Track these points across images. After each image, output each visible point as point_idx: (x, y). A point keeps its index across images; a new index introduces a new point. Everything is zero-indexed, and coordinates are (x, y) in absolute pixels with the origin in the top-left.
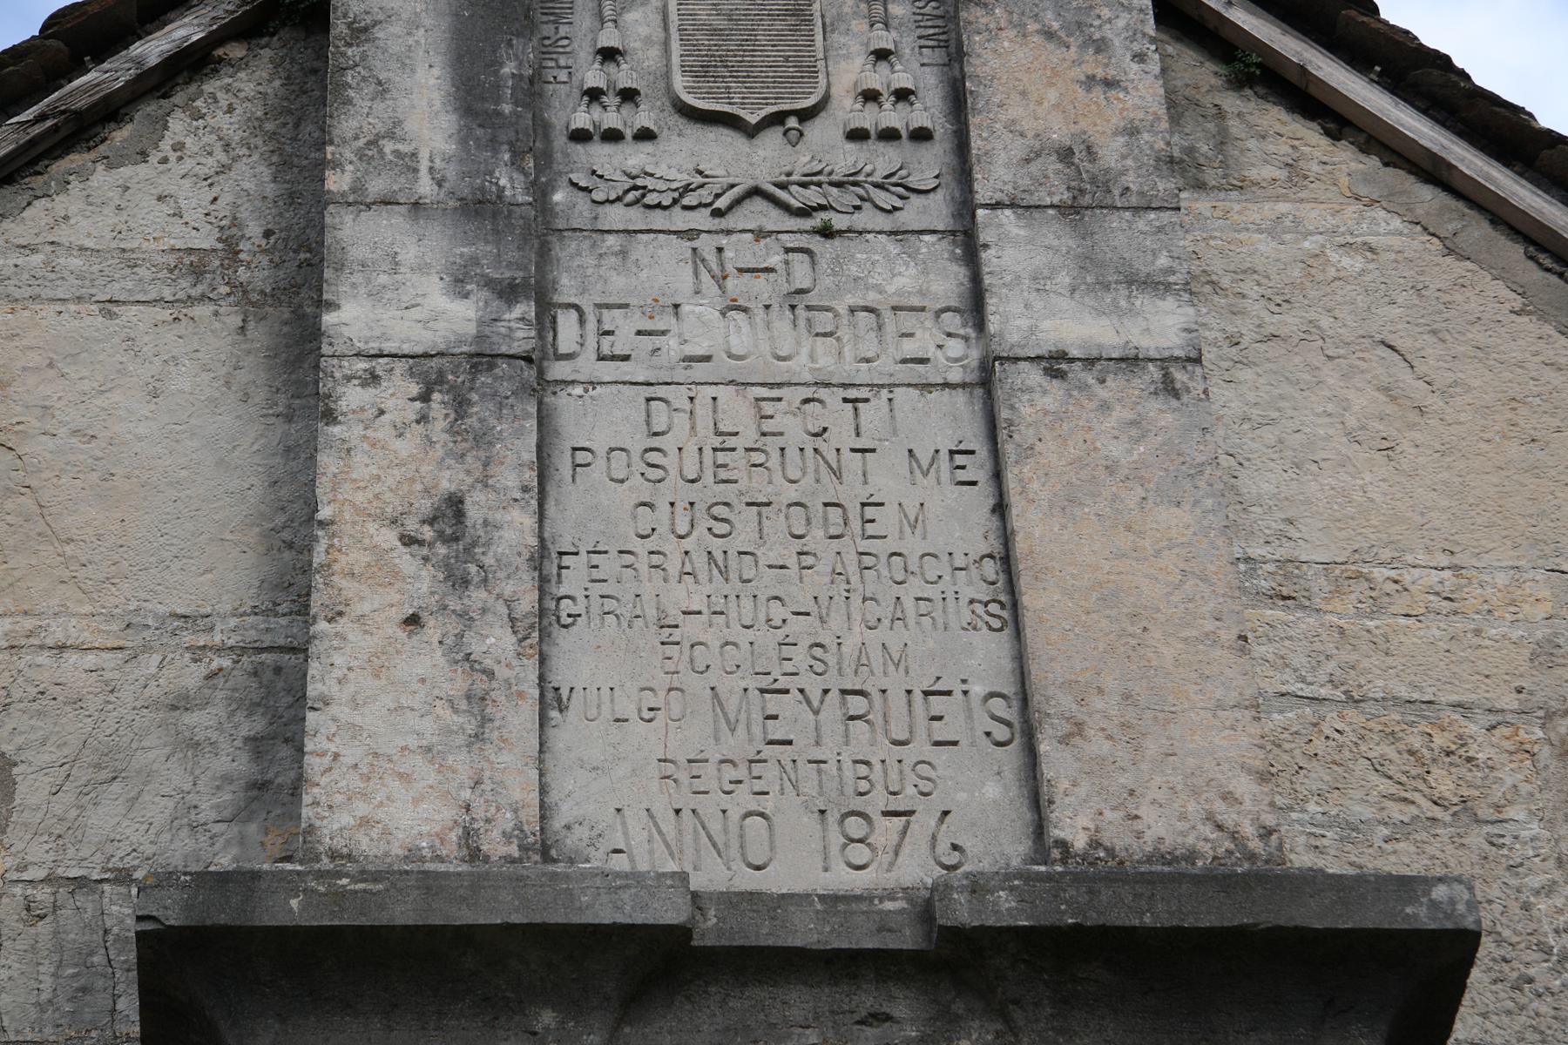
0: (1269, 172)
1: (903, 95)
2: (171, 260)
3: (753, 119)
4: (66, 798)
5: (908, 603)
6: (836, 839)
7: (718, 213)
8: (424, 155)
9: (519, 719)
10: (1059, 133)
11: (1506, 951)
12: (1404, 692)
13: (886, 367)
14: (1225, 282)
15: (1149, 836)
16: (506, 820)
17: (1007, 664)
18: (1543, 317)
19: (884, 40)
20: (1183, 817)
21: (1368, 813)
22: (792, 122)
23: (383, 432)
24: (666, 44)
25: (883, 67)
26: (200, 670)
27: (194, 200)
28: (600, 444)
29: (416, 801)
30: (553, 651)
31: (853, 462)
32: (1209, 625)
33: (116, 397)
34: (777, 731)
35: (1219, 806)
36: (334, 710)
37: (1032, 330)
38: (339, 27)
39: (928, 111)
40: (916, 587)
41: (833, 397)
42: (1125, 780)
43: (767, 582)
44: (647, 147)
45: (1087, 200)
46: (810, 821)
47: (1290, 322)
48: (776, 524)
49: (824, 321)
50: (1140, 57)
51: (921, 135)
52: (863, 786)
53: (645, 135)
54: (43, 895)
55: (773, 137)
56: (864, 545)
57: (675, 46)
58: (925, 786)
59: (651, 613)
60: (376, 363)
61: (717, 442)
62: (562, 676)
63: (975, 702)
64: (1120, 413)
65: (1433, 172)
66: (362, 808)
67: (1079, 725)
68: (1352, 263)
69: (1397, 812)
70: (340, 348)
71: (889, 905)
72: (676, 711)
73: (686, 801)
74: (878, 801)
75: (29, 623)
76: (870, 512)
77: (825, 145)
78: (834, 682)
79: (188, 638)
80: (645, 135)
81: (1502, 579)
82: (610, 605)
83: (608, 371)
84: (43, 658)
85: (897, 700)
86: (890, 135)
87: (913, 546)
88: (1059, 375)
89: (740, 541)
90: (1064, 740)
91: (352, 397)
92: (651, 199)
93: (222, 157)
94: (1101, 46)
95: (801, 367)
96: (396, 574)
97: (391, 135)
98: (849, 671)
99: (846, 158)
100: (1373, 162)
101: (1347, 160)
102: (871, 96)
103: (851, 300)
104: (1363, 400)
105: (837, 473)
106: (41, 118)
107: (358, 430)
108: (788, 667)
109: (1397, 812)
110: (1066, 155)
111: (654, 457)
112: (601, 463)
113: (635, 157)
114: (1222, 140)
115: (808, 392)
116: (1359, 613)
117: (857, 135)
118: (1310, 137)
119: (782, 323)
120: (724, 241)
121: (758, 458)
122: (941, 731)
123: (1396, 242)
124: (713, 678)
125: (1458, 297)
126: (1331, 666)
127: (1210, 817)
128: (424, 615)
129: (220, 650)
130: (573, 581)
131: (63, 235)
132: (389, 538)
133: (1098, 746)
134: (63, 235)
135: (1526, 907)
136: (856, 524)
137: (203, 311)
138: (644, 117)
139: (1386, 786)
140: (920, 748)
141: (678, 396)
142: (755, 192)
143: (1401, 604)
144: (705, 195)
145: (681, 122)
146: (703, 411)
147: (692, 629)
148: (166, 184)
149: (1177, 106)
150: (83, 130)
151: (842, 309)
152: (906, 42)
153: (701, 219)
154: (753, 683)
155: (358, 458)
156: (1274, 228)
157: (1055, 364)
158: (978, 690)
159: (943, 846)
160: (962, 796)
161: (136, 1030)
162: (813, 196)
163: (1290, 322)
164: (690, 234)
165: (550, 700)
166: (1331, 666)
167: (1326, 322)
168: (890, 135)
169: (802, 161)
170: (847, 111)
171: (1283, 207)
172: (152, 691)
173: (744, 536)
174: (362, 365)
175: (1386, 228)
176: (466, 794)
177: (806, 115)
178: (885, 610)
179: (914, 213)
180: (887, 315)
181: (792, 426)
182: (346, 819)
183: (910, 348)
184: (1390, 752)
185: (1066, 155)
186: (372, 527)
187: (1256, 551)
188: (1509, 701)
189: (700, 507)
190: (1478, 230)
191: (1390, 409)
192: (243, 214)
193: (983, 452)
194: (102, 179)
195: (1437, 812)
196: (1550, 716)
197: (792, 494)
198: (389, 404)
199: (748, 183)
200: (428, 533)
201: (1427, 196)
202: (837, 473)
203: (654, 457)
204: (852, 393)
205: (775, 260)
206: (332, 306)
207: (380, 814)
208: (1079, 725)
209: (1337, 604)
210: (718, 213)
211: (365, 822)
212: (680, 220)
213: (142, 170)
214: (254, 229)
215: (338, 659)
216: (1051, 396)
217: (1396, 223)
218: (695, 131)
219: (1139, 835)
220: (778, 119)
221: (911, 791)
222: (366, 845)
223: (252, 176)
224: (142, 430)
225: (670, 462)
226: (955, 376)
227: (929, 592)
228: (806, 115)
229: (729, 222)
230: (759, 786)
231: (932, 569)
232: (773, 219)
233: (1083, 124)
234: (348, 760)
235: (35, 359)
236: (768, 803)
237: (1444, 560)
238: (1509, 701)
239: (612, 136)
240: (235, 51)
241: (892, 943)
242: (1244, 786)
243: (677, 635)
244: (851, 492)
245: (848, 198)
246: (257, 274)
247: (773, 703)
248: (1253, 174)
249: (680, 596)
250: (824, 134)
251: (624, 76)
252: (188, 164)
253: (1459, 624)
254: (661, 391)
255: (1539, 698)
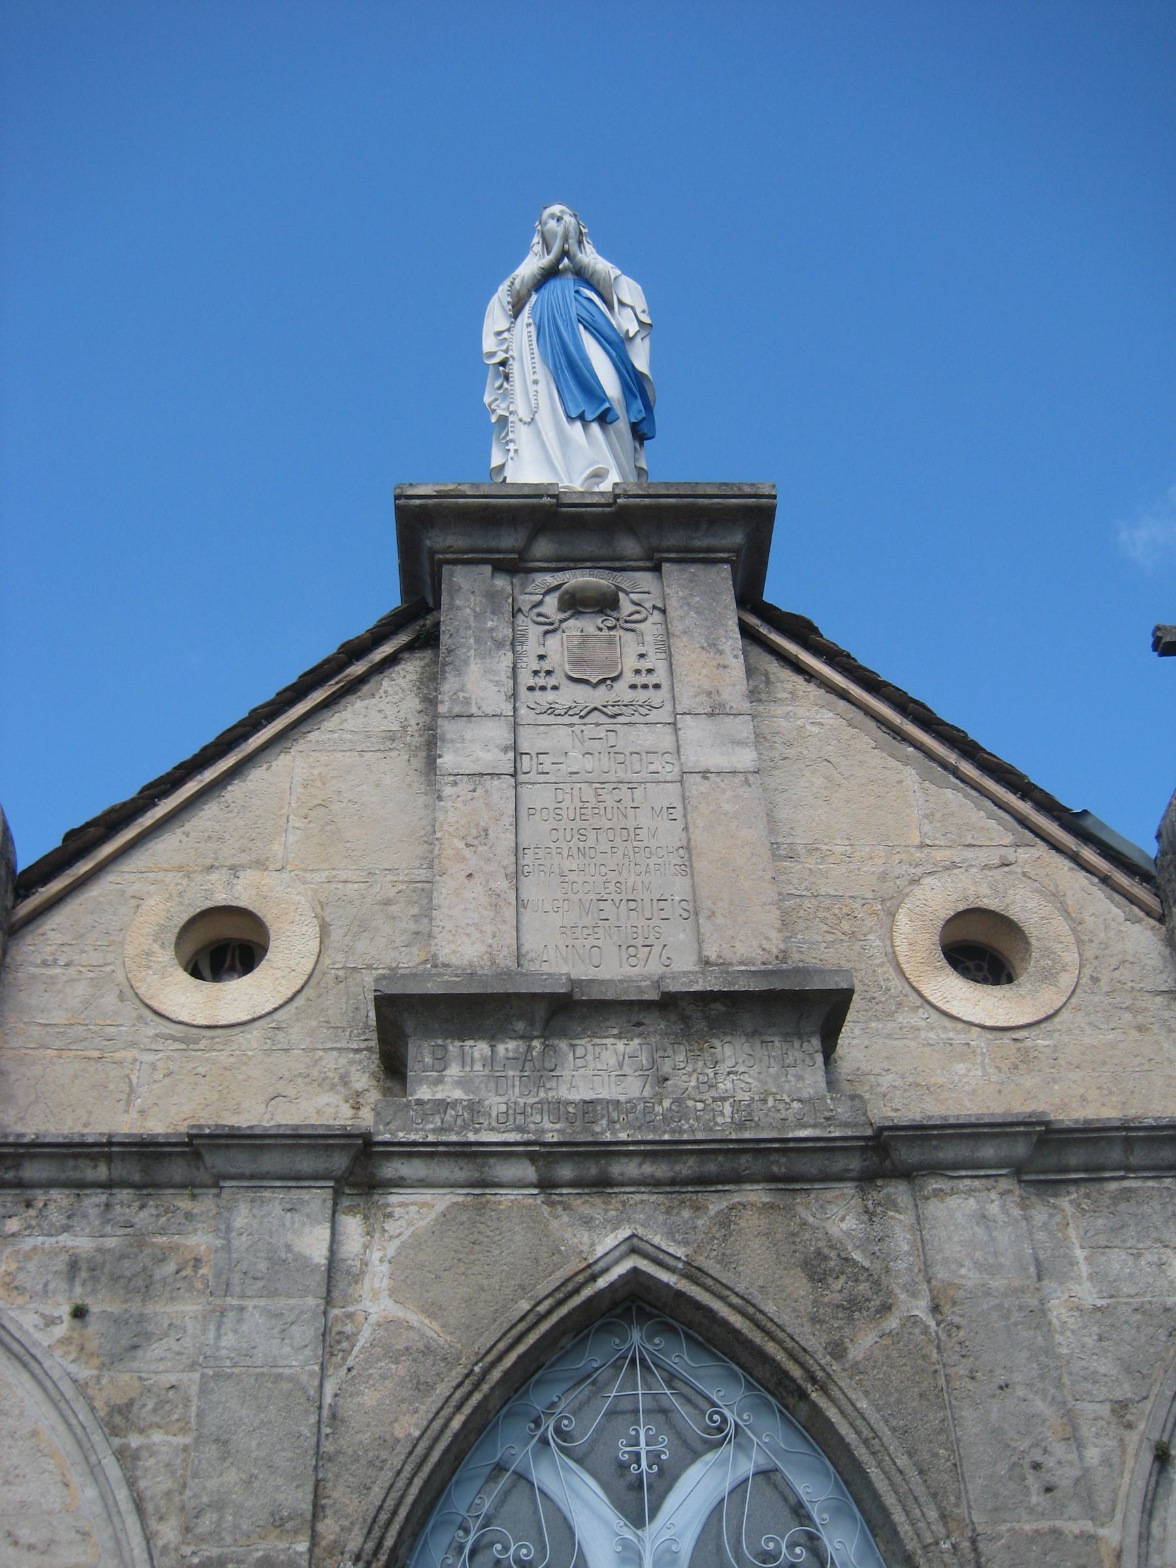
0: (785, 695)
1: (649, 671)
2: (383, 735)
3: (594, 681)
4: (348, 938)
5: (652, 866)
6: (625, 956)
7: (582, 717)
8: (473, 698)
9: (509, 913)
10: (707, 686)
11: (866, 988)
12: (832, 893)
13: (644, 775)
14: (769, 737)
15: (738, 954)
16: (505, 952)
17: (688, 889)
18: (883, 750)
19: (642, 650)
20: (751, 947)
21: (820, 939)
22: (609, 682)
23: (459, 805)
24: (562, 652)
25: (642, 660)
26: (395, 890)
27: (390, 711)
28: (538, 806)
29: (472, 944)
30: (521, 886)
31: (631, 812)
32: (761, 873)
33: (364, 787)
34: (603, 915)
35: (764, 942)
36: (442, 910)
37: (698, 761)
38: (443, 649)
39: (661, 676)
40: (654, 860)
41: (624, 787)
42: (731, 932)
43: (600, 859)
44: (555, 692)
45: (717, 711)
46: (616, 949)
47: (792, 752)
48: (603, 837)
49: (620, 758)
50: (736, 657)
51: (657, 686)
52: (635, 936)
53: (555, 688)
54: (341, 973)
55: (602, 688)
56: (636, 844)
57: (566, 653)
58: (658, 935)
59: (557, 871)
60: (456, 776)
61: (581, 805)
62: (524, 895)
63: (676, 902)
64: (729, 793)
65: (843, 695)
66: (453, 947)
67: (713, 912)
68: (815, 729)
69: (830, 938)
70: (443, 772)
71: (643, 984)
72: (566, 908)
73: (570, 942)
74: (640, 942)
75: (334, 872)
76: (638, 831)
77: (621, 691)
78: (624, 897)
79: (390, 878)
80: (555, 688)
81: (868, 849)
82: (542, 868)
83: (542, 778)
84: (340, 886)
85: (647, 904)
86: (645, 686)
87: (653, 844)
88: (707, 778)
89: (589, 843)
90: (709, 918)
91: (448, 791)
92: (557, 712)
93: (401, 695)
94: (721, 652)
95: (611, 777)
96: (464, 858)
97: (462, 691)
98: (630, 891)
99: (628, 696)
100: (823, 691)
101: (812, 690)
102: (638, 672)
103: (630, 750)
104: (819, 781)
105: (625, 816)
106: (337, 683)
107: (450, 803)
108: (608, 891)
109: (830, 938)
110: (709, 694)
111: (558, 811)
112: (538, 813)
113: (550, 696)
114: (768, 682)
115: (615, 785)
116: (817, 863)
117: (633, 687)
118: (799, 680)
119: (605, 758)
120: (584, 728)
121: (597, 811)
122: (663, 915)
123: (831, 722)
124: (580, 895)
125: (853, 742)
126: (806, 883)
127: (761, 946)
128: (475, 874)
129: (402, 882)
130: (528, 859)
131: (345, 726)
132: (460, 845)
133: (720, 920)
134: (345, 726)
135: (874, 971)
136: (632, 835)
137: (394, 754)
138: (552, 681)
139: (825, 928)
140: (656, 921)
141: (567, 787)
142: (595, 709)
143: (831, 859)
144: (576, 710)
145: (568, 682)
146: (576, 792)
147: (572, 877)
148: (382, 706)
149: (750, 671)
150: (353, 687)
151: (627, 754)
152: (649, 649)
153: (575, 719)
154: (595, 897)
155: (450, 814)
156: (787, 716)
157: (705, 774)
158: (677, 898)
159: (664, 957)
160: (671, 939)
161: (375, 1023)
162: (616, 710)
163: (792, 752)
164: (571, 725)
165: (520, 904)
166: (806, 883)
167: (805, 752)
168: (645, 686)
169: (612, 697)
170: (629, 678)
171: (790, 708)
172: (378, 898)
173: (591, 842)
174: (452, 778)
175: (827, 716)
176: (490, 941)
177: (614, 679)
178: (642, 869)
179: (654, 716)
180: (644, 755)
181: (609, 799)
182: (447, 951)
183: (652, 768)
184: (827, 915)
185: (709, 694)
186: (455, 840)
187: (780, 840)
188: (869, 895)
189: (575, 831)
190: (859, 716)
191: (829, 785)
192: (409, 717)
193: (680, 807)
194: (359, 704)
195: (843, 937)
196: (883, 901)
197: (609, 824)
198: (461, 793)
199: (593, 706)
200: (475, 842)
201: (842, 704)
202: (625, 816)
203: (558, 811)
204: (631, 786)
205: (602, 735)
206: (440, 756)
207: (459, 949)
208: (713, 912)
209: (809, 860)
210: (582, 717)
211: (454, 952)
212: (566, 719)
213: (373, 701)
214: (413, 722)
215: (444, 891)
216: (705, 786)
217: (831, 714)
218: (573, 686)
219: (735, 953)
220: (604, 681)
221: (652, 937)
222: (454, 960)
223: (412, 703)
224: (373, 799)
225: (564, 813)
226: (669, 778)
227: (660, 861)
228: (614, 679)
229: (585, 721)
230: (597, 936)
231: (661, 853)
232: (603, 719)
233: (716, 682)
234: (447, 929)
235: (335, 773)
236: (600, 943)
237: (847, 842)
238: (869, 895)
239: (543, 688)
240: (406, 655)
241: (646, 997)
242: (773, 934)
243: (567, 879)
244: (631, 824)
245: (629, 710)
246: (417, 740)
247: (602, 905)
248: (779, 696)
249: (568, 864)
250: (621, 686)
251: (546, 665)
252: (389, 698)
253: (852, 867)
254: (560, 786)
255: (880, 894)
